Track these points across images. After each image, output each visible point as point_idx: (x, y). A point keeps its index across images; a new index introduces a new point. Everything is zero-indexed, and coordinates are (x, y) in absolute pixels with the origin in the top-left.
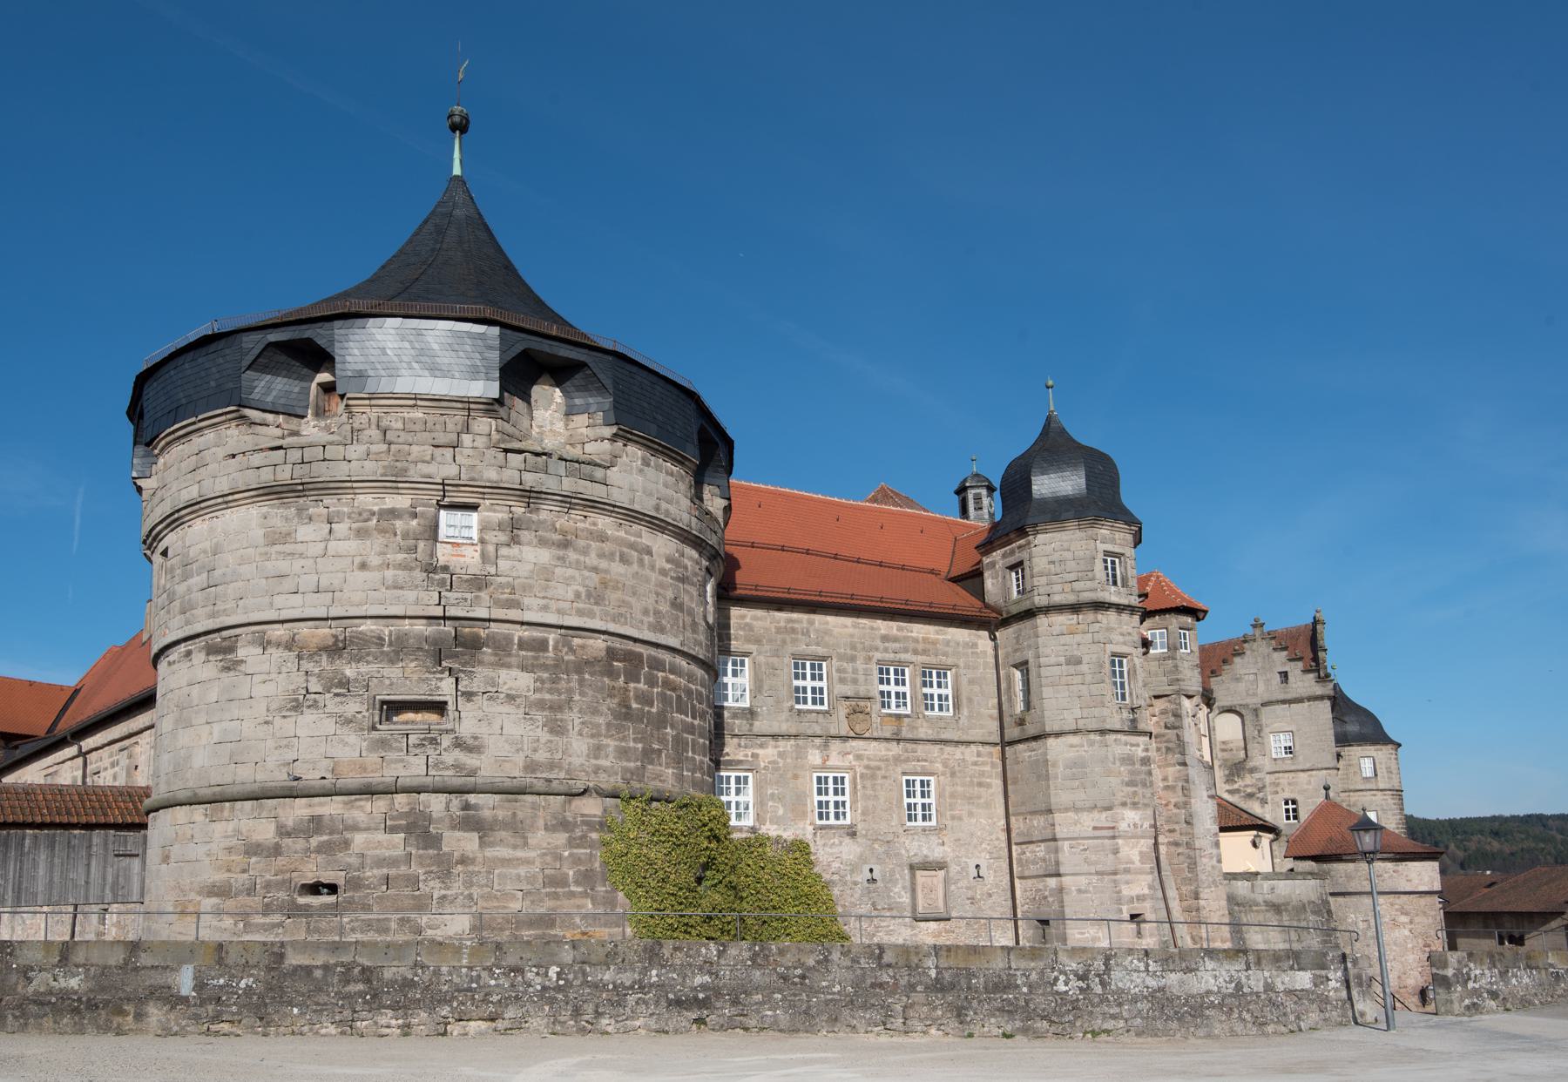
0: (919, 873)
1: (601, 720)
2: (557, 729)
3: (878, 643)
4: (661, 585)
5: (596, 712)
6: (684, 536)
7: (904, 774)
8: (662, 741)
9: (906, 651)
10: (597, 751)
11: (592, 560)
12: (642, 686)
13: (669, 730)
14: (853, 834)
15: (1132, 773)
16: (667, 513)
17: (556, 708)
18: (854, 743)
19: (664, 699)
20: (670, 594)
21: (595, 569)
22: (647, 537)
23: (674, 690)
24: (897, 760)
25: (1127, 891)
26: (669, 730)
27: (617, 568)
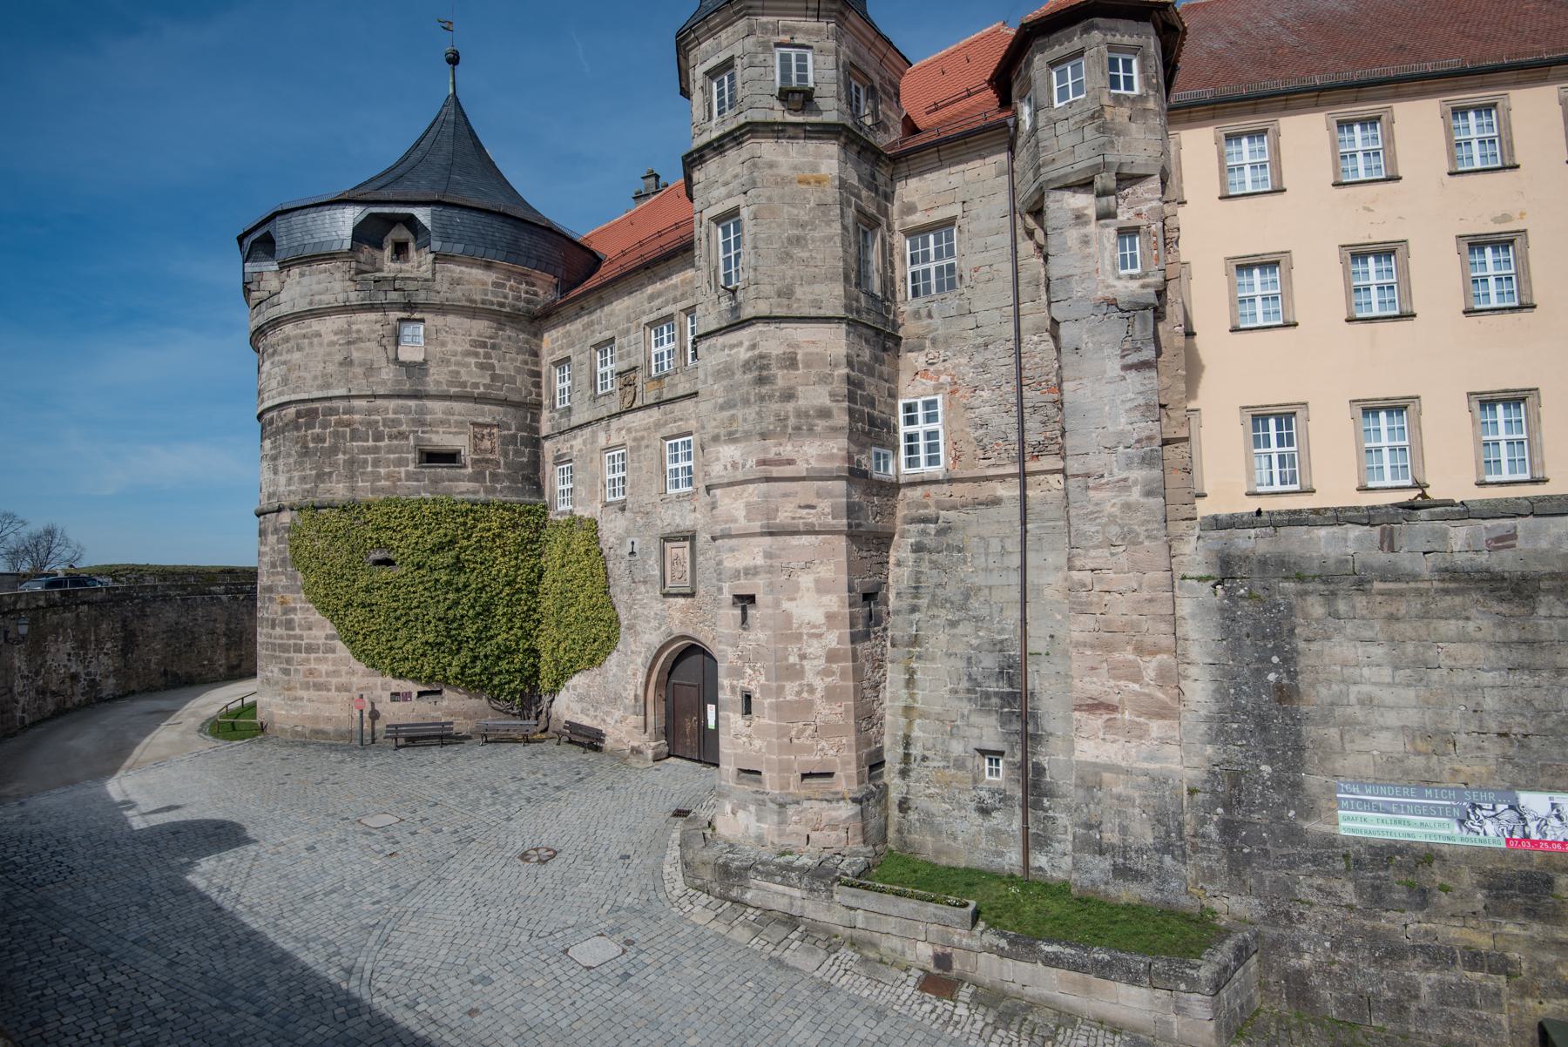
0: (668, 545)
1: (291, 460)
2: (276, 472)
3: (647, 306)
4: (329, 354)
5: (289, 455)
6: (346, 309)
7: (666, 438)
8: (334, 465)
9: (667, 303)
10: (290, 481)
11: (283, 358)
12: (317, 430)
13: (341, 456)
14: (623, 509)
15: (730, 389)
16: (321, 302)
17: (274, 458)
18: (626, 418)
19: (336, 434)
20: (339, 358)
21: (285, 363)
22: (315, 325)
23: (348, 426)
24: (658, 425)
25: (729, 563)
26: (341, 456)
27: (297, 356)
